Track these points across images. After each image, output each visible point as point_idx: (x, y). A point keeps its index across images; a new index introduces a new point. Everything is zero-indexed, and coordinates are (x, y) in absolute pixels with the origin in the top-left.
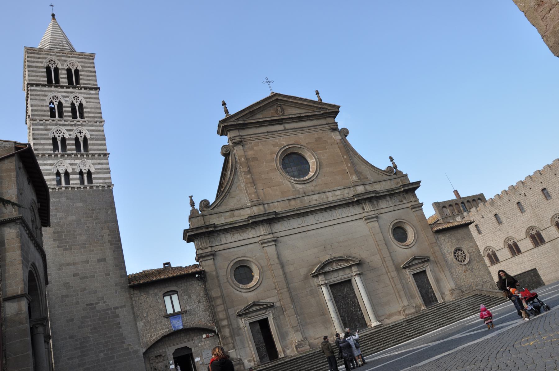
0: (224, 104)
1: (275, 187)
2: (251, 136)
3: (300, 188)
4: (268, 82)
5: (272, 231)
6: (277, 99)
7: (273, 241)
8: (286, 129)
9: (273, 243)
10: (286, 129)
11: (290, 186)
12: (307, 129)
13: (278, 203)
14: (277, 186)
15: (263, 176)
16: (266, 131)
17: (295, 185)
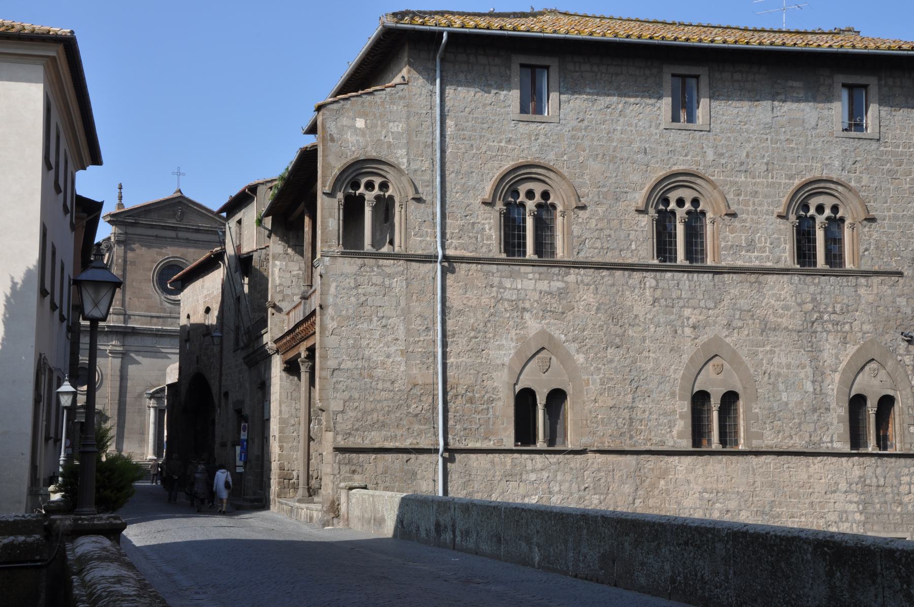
0: (121, 188)
1: (143, 299)
2: (138, 237)
3: (168, 307)
4: (179, 174)
5: (123, 342)
6: (180, 202)
7: (121, 353)
8: (177, 238)
9: (121, 356)
10: (177, 238)
11: (159, 301)
12: (201, 243)
13: (140, 317)
14: (144, 298)
15: (134, 284)
16: (155, 234)
17: (164, 302)
